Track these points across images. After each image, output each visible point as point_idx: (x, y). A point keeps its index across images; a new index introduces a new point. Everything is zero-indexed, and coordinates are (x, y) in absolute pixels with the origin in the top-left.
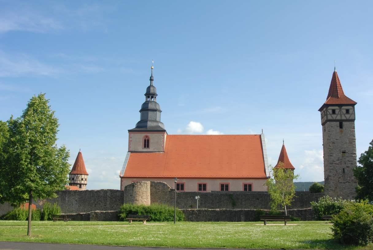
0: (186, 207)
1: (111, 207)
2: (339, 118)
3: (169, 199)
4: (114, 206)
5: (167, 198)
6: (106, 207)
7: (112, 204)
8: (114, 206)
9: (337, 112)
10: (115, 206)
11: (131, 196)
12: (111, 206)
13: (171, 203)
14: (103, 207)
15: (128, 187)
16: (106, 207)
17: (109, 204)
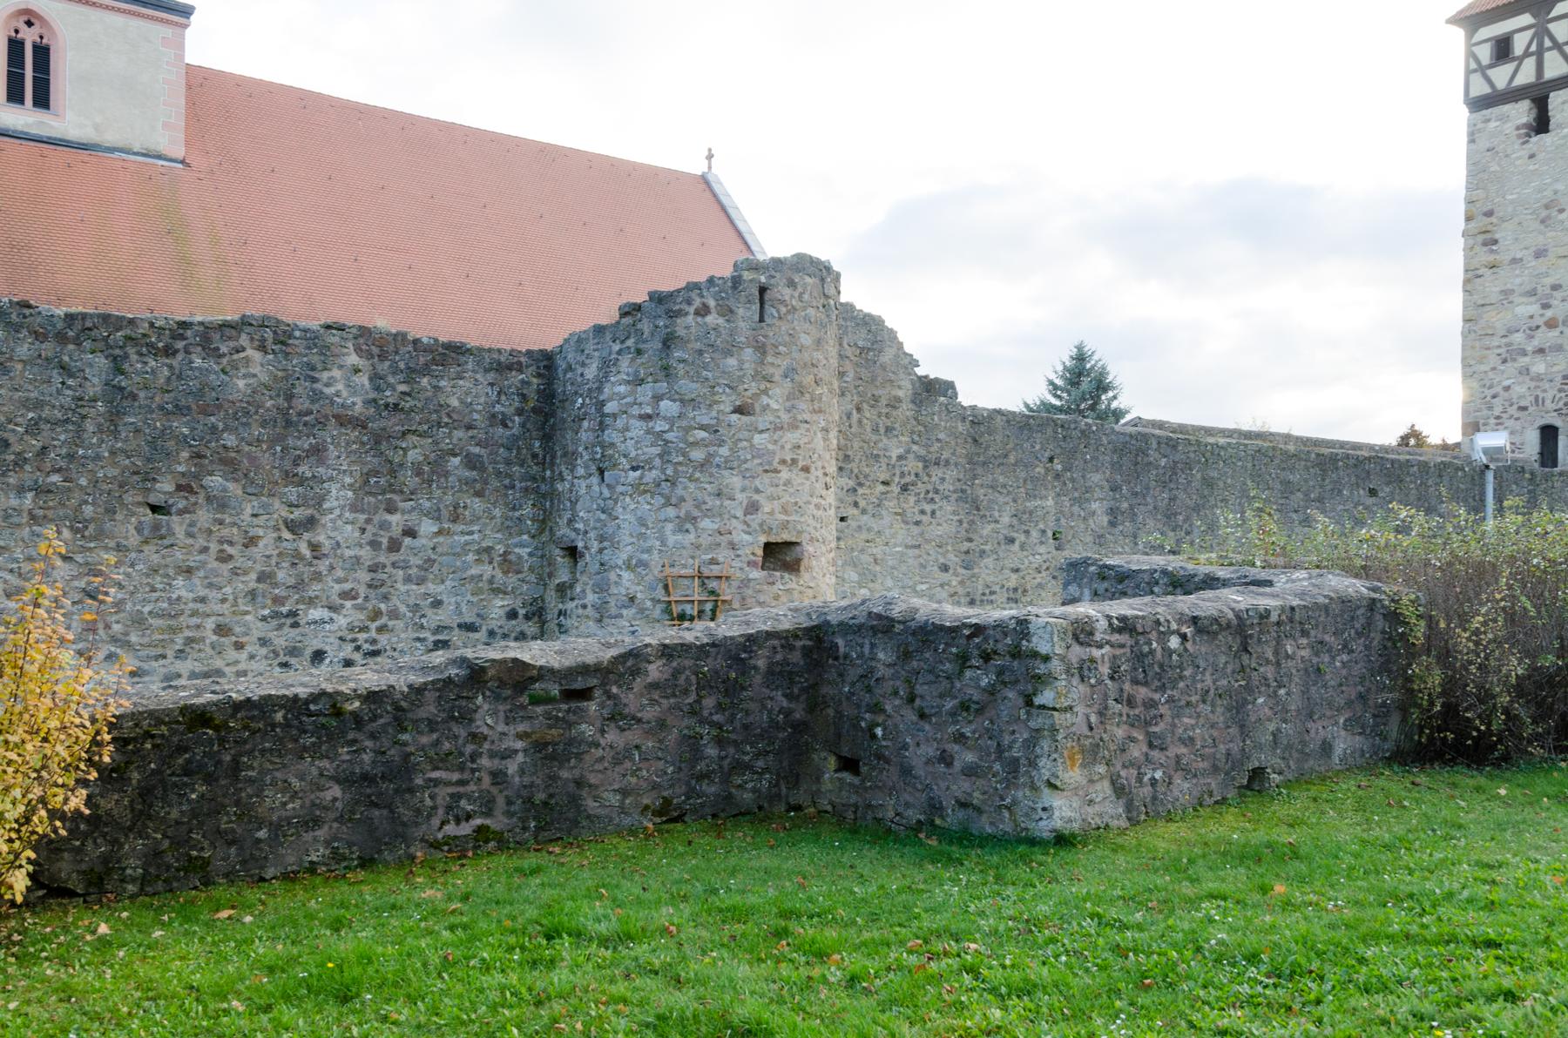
0: (1022, 538)
1: (375, 544)
2: (1526, 75)
3: (913, 465)
4: (411, 533)
5: (900, 458)
6: (314, 547)
7: (391, 509)
8: (411, 533)
9: (1519, 44)
10: (427, 527)
11: (739, 410)
12: (384, 526)
13: (928, 508)
14: (267, 544)
15: (703, 311)
16: (314, 547)
17: (354, 508)
